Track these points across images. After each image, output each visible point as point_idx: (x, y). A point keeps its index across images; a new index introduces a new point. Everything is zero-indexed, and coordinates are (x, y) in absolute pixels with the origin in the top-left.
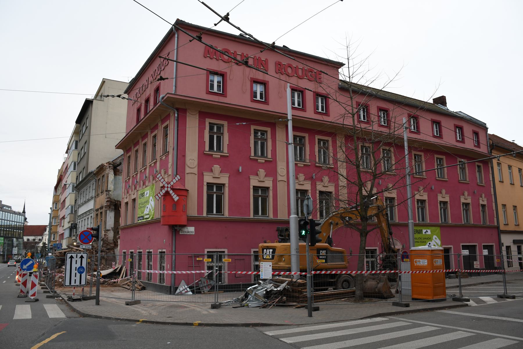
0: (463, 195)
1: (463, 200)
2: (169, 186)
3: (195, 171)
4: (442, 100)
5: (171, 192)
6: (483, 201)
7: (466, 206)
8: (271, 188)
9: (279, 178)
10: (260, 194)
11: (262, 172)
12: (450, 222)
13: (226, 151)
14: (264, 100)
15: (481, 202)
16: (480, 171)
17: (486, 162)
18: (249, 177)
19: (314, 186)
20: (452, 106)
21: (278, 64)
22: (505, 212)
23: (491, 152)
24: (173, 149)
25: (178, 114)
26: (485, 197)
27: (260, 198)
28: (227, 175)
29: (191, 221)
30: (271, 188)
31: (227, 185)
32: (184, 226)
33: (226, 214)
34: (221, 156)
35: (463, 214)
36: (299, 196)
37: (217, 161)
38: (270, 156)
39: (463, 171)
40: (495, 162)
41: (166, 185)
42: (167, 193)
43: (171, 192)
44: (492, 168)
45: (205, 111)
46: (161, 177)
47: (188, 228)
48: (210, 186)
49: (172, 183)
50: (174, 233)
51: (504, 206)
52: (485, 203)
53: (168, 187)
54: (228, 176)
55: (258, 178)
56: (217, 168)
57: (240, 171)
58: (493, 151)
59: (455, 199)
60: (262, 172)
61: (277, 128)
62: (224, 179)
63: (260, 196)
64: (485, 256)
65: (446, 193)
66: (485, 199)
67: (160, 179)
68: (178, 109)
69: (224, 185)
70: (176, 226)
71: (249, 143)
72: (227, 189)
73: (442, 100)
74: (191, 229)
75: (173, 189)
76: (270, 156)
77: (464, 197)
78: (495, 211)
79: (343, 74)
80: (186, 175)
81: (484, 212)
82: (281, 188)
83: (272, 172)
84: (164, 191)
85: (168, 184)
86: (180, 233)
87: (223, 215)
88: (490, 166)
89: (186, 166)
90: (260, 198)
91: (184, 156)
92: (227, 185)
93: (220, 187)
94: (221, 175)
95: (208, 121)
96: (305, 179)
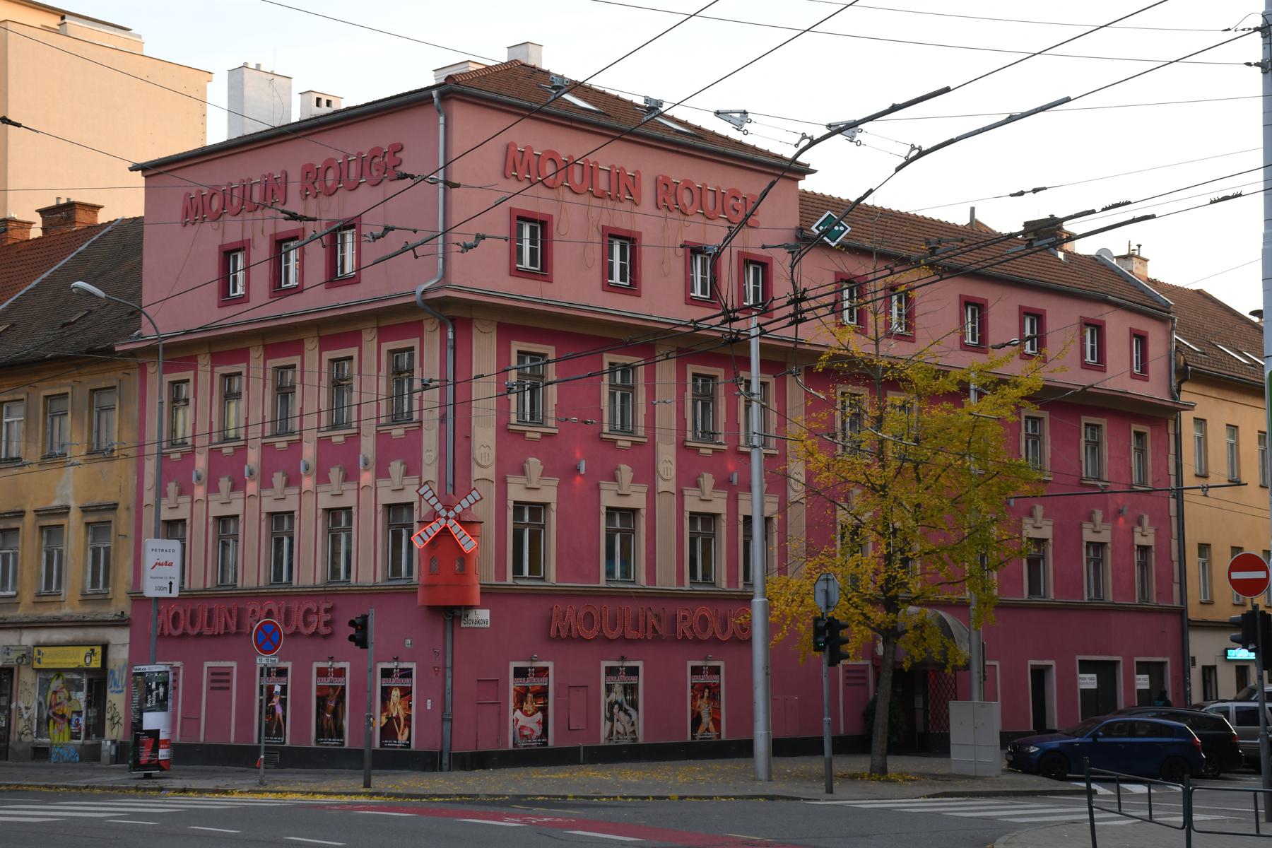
0: (1090, 519)
1: (1088, 536)
2: (451, 514)
3: (491, 473)
5: (456, 529)
6: (1144, 536)
7: (1096, 553)
8: (643, 512)
9: (661, 486)
10: (618, 525)
11: (626, 472)
12: (1052, 596)
13: (551, 423)
15: (1139, 540)
16: (1141, 451)
17: (1159, 416)
18: (598, 485)
19: (733, 502)
21: (663, 184)
22: (1206, 566)
23: (1179, 391)
24: (443, 419)
26: (1151, 524)
27: (618, 536)
28: (555, 482)
29: (491, 595)
30: (643, 512)
31: (554, 507)
32: (471, 607)
33: (552, 576)
34: (543, 434)
35: (1086, 568)
36: (699, 528)
37: (533, 448)
38: (641, 431)
39: (1093, 450)
40: (1187, 418)
41: (443, 513)
42: (445, 531)
43: (456, 529)
44: (1178, 438)
45: (515, 323)
46: (430, 493)
47: (478, 611)
48: (519, 506)
49: (458, 509)
50: (449, 625)
51: (1204, 548)
52: (1149, 541)
53: (447, 518)
54: (556, 483)
55: (616, 487)
58: (1184, 386)
60: (626, 472)
62: (548, 493)
63: (618, 531)
65: (1045, 516)
66: (1150, 531)
67: (427, 497)
68: (453, 320)
69: (546, 505)
70: (459, 608)
71: (599, 400)
72: (553, 516)
74: (484, 615)
75: (459, 519)
76: (641, 431)
77: (1091, 526)
78: (1176, 565)
81: (1144, 565)
82: (666, 508)
83: (646, 474)
84: (436, 527)
85: (448, 510)
87: (543, 579)
88: (1171, 430)
89: (473, 463)
90: (618, 536)
91: (468, 438)
92: (554, 507)
93: (538, 509)
94: (543, 482)
95: (516, 346)
96: (717, 486)
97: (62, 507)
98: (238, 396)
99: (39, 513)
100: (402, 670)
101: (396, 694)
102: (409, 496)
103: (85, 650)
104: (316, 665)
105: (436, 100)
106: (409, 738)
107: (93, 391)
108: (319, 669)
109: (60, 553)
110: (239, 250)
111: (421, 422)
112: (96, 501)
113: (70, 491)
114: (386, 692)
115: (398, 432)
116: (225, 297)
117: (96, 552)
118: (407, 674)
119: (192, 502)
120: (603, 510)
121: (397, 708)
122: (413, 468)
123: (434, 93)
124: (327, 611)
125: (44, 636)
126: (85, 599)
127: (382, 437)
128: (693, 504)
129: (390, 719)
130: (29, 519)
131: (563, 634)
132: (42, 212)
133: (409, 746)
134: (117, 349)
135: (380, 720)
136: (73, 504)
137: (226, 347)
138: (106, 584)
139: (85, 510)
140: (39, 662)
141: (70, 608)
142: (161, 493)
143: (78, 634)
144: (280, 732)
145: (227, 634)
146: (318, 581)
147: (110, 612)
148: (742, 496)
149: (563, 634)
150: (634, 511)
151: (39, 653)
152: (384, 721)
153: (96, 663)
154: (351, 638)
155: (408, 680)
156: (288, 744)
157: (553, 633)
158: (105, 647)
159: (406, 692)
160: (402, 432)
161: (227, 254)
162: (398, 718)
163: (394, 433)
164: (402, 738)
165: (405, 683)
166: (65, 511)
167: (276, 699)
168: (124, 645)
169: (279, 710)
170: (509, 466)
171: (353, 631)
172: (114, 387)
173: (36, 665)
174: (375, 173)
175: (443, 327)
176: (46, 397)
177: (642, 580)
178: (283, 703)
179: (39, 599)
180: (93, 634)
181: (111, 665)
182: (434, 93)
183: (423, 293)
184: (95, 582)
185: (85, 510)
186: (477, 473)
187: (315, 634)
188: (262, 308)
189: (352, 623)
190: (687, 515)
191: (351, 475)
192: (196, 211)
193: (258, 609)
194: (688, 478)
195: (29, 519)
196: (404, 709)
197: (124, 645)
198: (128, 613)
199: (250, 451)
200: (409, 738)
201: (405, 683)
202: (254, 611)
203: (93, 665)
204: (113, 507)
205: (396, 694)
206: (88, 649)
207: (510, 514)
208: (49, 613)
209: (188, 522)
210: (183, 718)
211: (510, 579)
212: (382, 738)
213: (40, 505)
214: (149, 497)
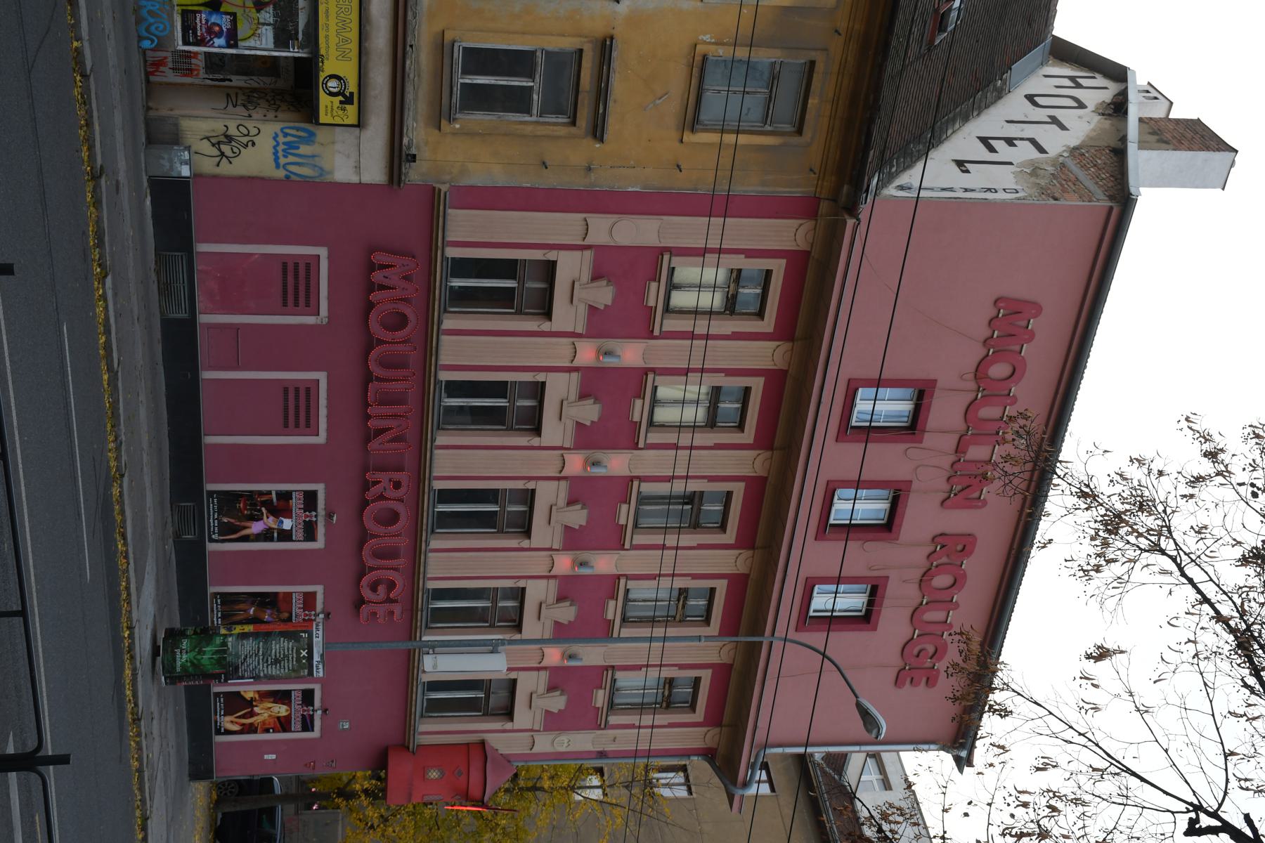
100: (312, 717)
101: (282, 710)
103: (349, 70)
104: (319, 589)
106: (228, 732)
108: (314, 594)
114: (283, 697)
118: (307, 725)
121: (267, 711)
129: (250, 703)
133: (218, 732)
135: (249, 691)
143: (380, 40)
144: (228, 531)
145: (369, 436)
147: (417, 132)
152: (248, 696)
155: (299, 726)
156: (211, 547)
159: (284, 724)
162: (252, 714)
164: (228, 722)
165: (296, 724)
167: (271, 522)
168: (358, 168)
169: (256, 528)
178: (267, 536)
180: (380, 77)
193: (400, 492)
194: (581, 490)
196: (264, 723)
197: (358, 168)
198: (414, 174)
200: (228, 732)
201: (296, 724)
202: (397, 485)
205: (282, 710)
206: (352, 87)
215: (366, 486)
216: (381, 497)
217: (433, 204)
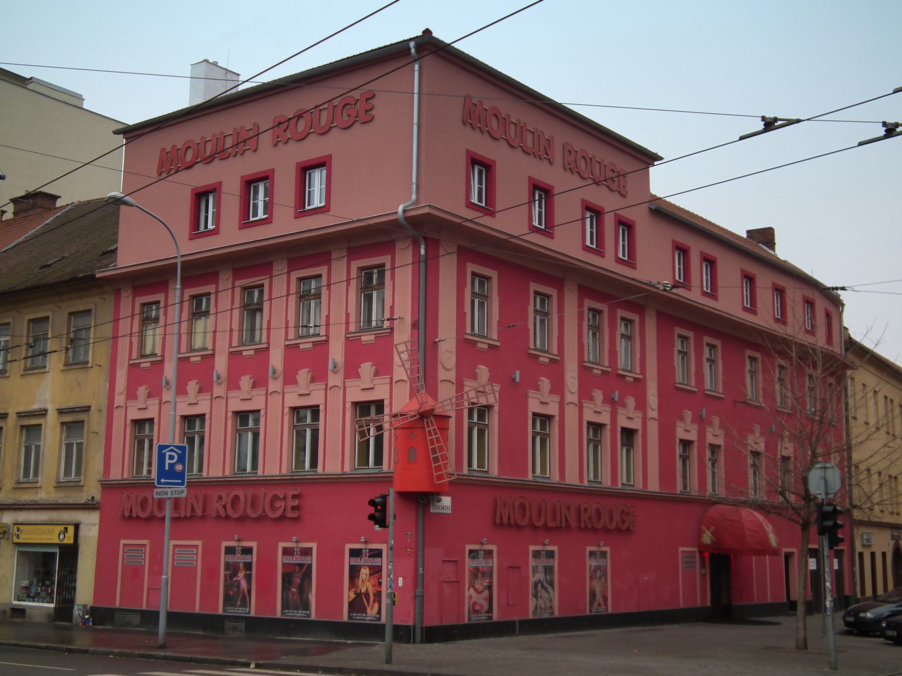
3: (452, 375)
4: (766, 236)
11: (545, 383)
14: (543, 227)
20: (783, 251)
21: (568, 150)
25: (426, 251)
31: (496, 409)
38: (555, 351)
47: (443, 498)
55: (539, 396)
56: (483, 371)
57: (518, 380)
59: (771, 447)
61: (566, 291)
63: (538, 433)
64: (812, 571)
68: (425, 238)
73: (766, 236)
79: (662, 183)
80: (439, 384)
83: (558, 388)
86: (432, 511)
97: (40, 410)
98: (206, 313)
99: (20, 415)
100: (371, 550)
101: (365, 572)
102: (380, 392)
104: (281, 545)
105: (413, 50)
106: (379, 612)
107: (71, 314)
109: (38, 447)
110: (211, 192)
111: (392, 329)
112: (71, 404)
113: (48, 396)
114: (354, 572)
115: (368, 338)
116: (196, 230)
117: (69, 446)
118: (378, 554)
119: (160, 404)
120: (530, 415)
121: (365, 583)
122: (383, 368)
123: (412, 44)
124: (294, 497)
125: (22, 516)
126: (59, 486)
127: (351, 343)
128: (589, 416)
129: (359, 595)
130: (12, 419)
131: (505, 521)
132: (14, 201)
133: (379, 619)
134: (98, 276)
135: (348, 595)
136: (51, 408)
137: (201, 271)
138: (78, 473)
139: (61, 412)
140: (18, 537)
141: (44, 495)
142: (131, 395)
144: (245, 602)
146: (284, 471)
147: (82, 497)
148: (620, 410)
149: (505, 521)
150: (550, 418)
151: (18, 530)
152: (353, 596)
153: (69, 540)
154: (371, 517)
155: (378, 560)
156: (253, 614)
157: (498, 521)
158: (77, 527)
159: (376, 571)
160: (373, 337)
161: (200, 196)
162: (367, 594)
163: (363, 338)
164: (372, 612)
165: (376, 562)
166: (43, 413)
167: (241, 575)
168: (94, 525)
169: (244, 584)
170: (464, 371)
171: (372, 510)
172: (90, 310)
173: (16, 540)
174: (346, 118)
175: (416, 245)
176: (30, 320)
177: (556, 478)
178: (248, 578)
179: (18, 487)
181: (81, 541)
182: (412, 44)
183: (404, 211)
184: (67, 472)
185: (61, 412)
186: (442, 375)
187: (283, 518)
188: (231, 237)
189: (372, 503)
190: (585, 423)
191: (319, 376)
192: (170, 165)
195: (12, 419)
196: (374, 586)
197: (94, 525)
198: (98, 497)
199: (217, 358)
200: (379, 612)
202: (220, 498)
203: (66, 541)
204: (87, 409)
205: (365, 572)
206: (62, 528)
207: (466, 412)
208: (26, 497)
209: (156, 420)
210: (149, 589)
211: (465, 471)
212: (283, 608)
213: (22, 409)
214: (119, 400)
215: (218, 517)
216: (225, 507)
217: (107, 487)
